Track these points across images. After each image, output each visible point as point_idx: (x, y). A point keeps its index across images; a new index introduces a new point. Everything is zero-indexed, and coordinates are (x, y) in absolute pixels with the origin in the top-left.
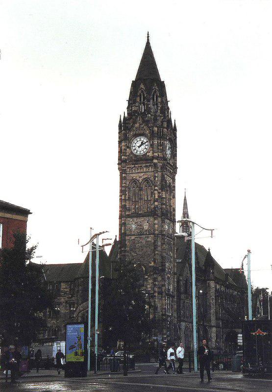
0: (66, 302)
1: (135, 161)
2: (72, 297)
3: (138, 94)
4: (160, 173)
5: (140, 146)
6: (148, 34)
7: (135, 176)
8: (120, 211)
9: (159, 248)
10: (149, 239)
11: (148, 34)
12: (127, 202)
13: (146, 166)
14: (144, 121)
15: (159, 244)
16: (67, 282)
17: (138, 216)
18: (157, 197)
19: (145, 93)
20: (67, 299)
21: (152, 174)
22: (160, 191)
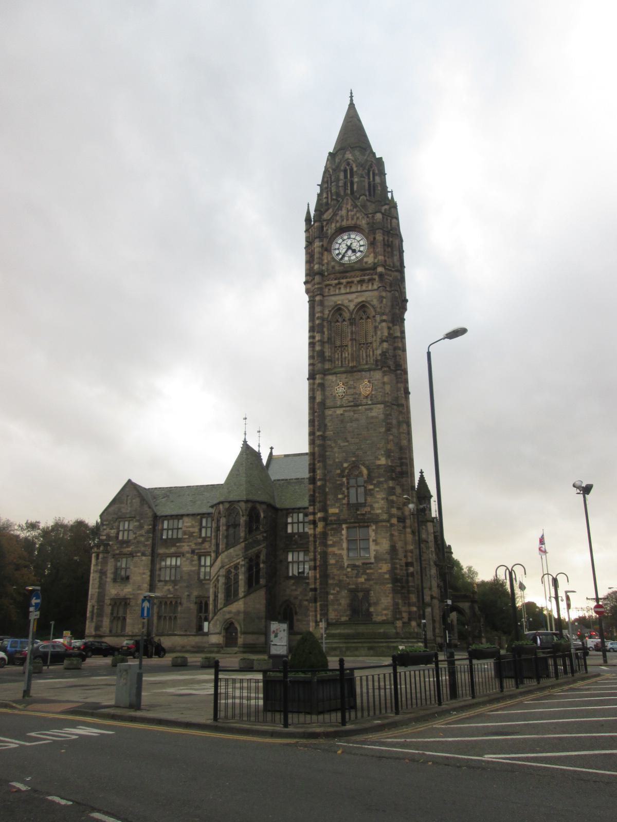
0: (193, 552)
3: (342, 168)
4: (389, 294)
5: (351, 247)
6: (351, 93)
7: (339, 300)
8: (310, 365)
9: (394, 431)
10: (374, 414)
11: (351, 93)
12: (327, 346)
13: (361, 282)
14: (355, 206)
15: (394, 422)
16: (193, 515)
17: (351, 371)
18: (386, 334)
19: (354, 166)
20: (194, 546)
21: (376, 293)
22: (391, 325)
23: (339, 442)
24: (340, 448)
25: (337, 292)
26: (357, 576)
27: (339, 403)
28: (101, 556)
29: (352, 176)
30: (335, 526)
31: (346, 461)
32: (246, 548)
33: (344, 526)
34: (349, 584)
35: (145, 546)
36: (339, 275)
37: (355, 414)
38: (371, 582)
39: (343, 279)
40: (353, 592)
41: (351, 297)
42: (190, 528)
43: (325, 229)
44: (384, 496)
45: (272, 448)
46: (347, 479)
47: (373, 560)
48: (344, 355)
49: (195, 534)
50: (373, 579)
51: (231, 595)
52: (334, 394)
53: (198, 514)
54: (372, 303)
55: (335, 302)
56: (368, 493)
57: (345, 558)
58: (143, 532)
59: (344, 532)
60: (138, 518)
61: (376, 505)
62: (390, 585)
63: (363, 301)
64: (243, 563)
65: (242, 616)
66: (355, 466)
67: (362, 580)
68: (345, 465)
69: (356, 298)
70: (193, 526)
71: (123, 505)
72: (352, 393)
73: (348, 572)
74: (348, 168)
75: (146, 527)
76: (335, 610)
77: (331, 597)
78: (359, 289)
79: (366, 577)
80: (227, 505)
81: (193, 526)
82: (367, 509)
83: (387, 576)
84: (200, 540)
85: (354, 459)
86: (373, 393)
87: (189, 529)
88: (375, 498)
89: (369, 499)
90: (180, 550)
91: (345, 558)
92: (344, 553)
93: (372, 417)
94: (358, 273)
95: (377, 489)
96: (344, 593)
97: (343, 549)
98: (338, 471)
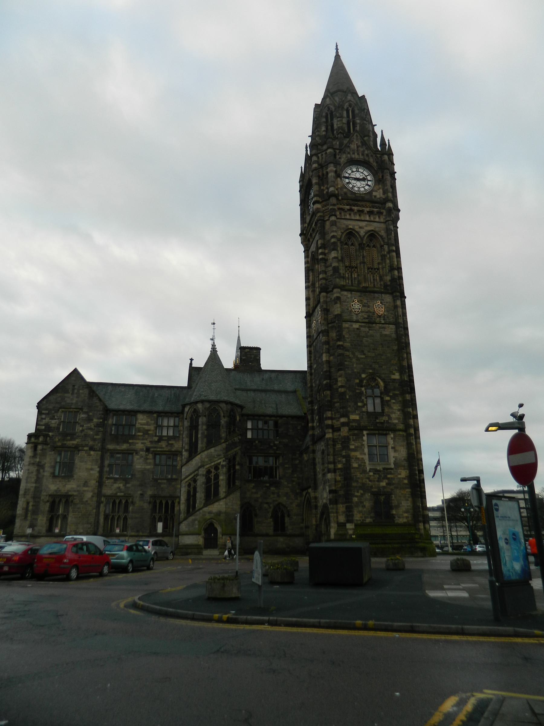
0: (148, 450)
1: (352, 200)
2: (159, 441)
3: (345, 107)
6: (337, 46)
7: (351, 224)
10: (387, 332)
13: (370, 213)
20: (149, 445)
23: (357, 354)
24: (358, 359)
25: (348, 217)
26: (379, 480)
27: (355, 318)
28: (40, 447)
29: (354, 117)
30: (356, 432)
31: (364, 372)
32: (227, 449)
33: (365, 432)
34: (372, 487)
35: (94, 440)
36: (351, 202)
37: (370, 330)
38: (392, 487)
39: (354, 206)
40: (376, 495)
41: (363, 224)
42: (144, 425)
43: (338, 157)
44: (399, 408)
45: (192, 360)
46: (366, 389)
47: (392, 466)
48: (353, 276)
49: (150, 432)
50: (393, 484)
51: (212, 495)
52: (350, 309)
53: (156, 412)
54: (380, 233)
55: (347, 226)
56: (384, 403)
57: (367, 462)
58: (92, 425)
59: (365, 438)
60: (85, 410)
61: (393, 416)
62: (409, 490)
63: (372, 230)
64: (224, 463)
65: (222, 517)
66: (372, 378)
67: (383, 484)
68: (363, 376)
69: (366, 226)
70: (148, 424)
71: (66, 395)
72: (367, 310)
73: (371, 476)
74: (350, 109)
75: (95, 420)
76: (360, 512)
77: (355, 499)
78: (368, 218)
79: (387, 481)
80: (207, 405)
81: (148, 424)
82: (385, 418)
83: (406, 481)
84: (156, 439)
85: (371, 371)
86: (385, 313)
87: (144, 427)
88: (392, 408)
89: (386, 410)
90: (133, 447)
91: (367, 462)
92: (366, 457)
93: (386, 335)
94: (368, 204)
95: (394, 401)
96: (368, 496)
97: (365, 454)
98: (357, 381)
